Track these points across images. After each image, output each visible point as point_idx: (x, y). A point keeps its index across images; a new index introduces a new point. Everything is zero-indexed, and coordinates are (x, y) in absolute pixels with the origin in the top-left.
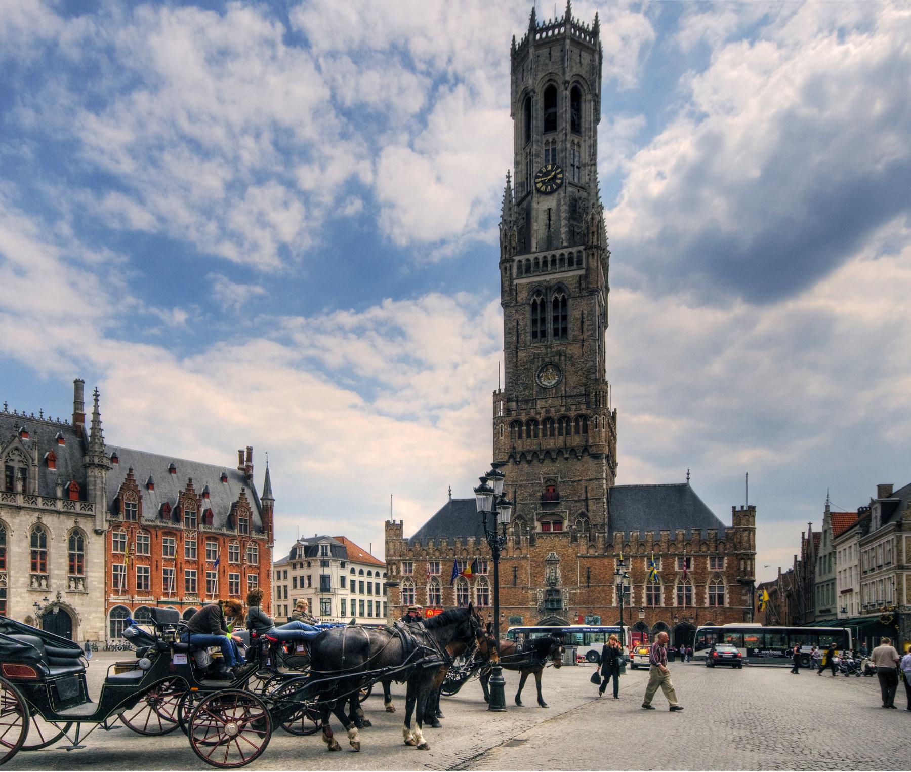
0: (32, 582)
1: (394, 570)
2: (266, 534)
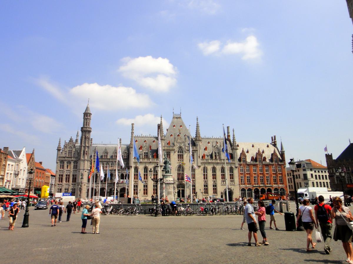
0: (222, 183)
1: (331, 171)
2: (283, 162)
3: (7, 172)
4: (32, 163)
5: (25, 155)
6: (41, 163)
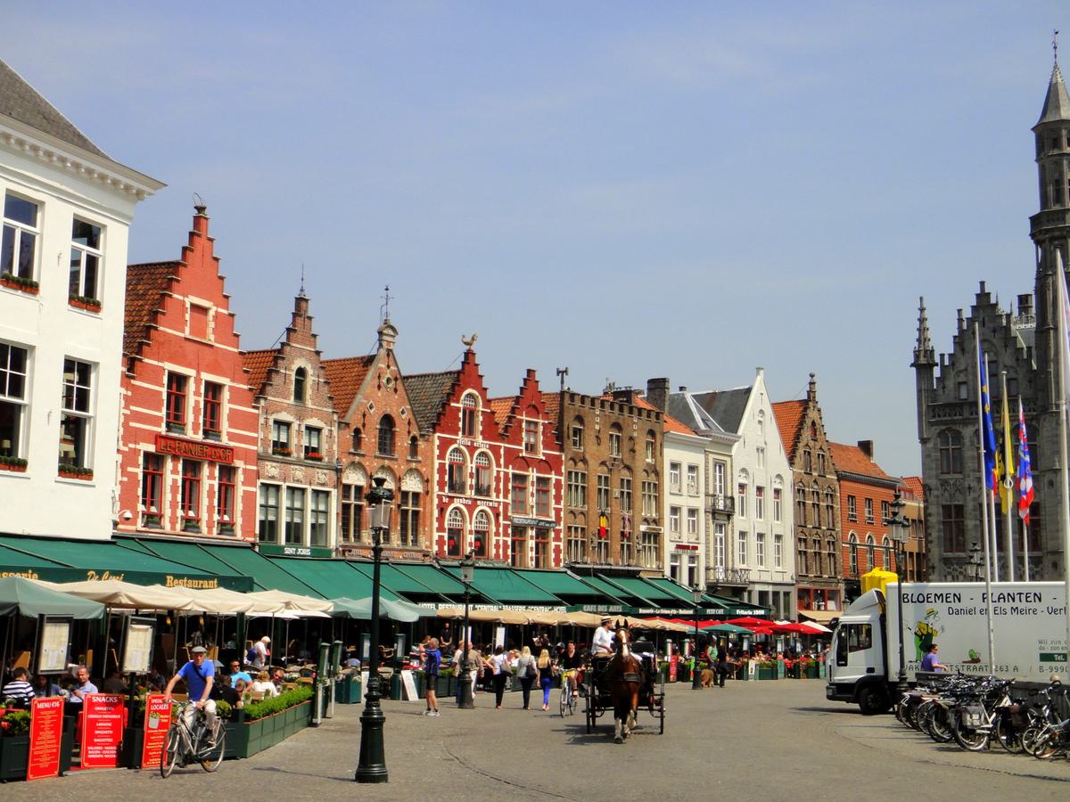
3: (669, 501)
4: (815, 453)
5: (769, 411)
6: (866, 447)
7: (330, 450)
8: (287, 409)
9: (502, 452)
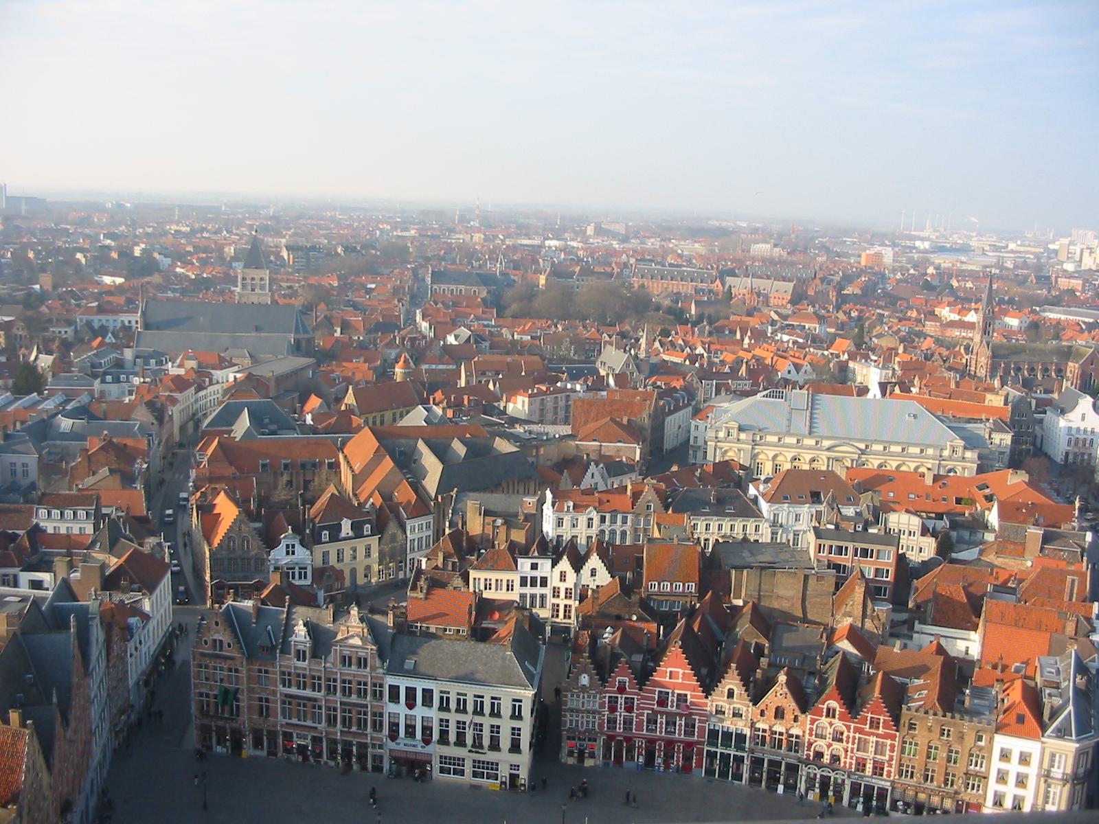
7: (747, 716)
8: (724, 701)
9: (852, 727)
